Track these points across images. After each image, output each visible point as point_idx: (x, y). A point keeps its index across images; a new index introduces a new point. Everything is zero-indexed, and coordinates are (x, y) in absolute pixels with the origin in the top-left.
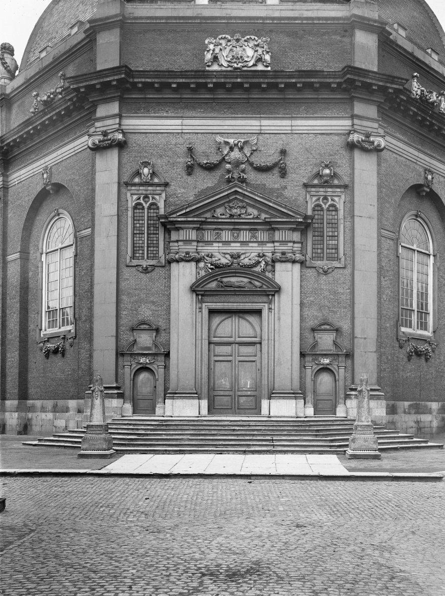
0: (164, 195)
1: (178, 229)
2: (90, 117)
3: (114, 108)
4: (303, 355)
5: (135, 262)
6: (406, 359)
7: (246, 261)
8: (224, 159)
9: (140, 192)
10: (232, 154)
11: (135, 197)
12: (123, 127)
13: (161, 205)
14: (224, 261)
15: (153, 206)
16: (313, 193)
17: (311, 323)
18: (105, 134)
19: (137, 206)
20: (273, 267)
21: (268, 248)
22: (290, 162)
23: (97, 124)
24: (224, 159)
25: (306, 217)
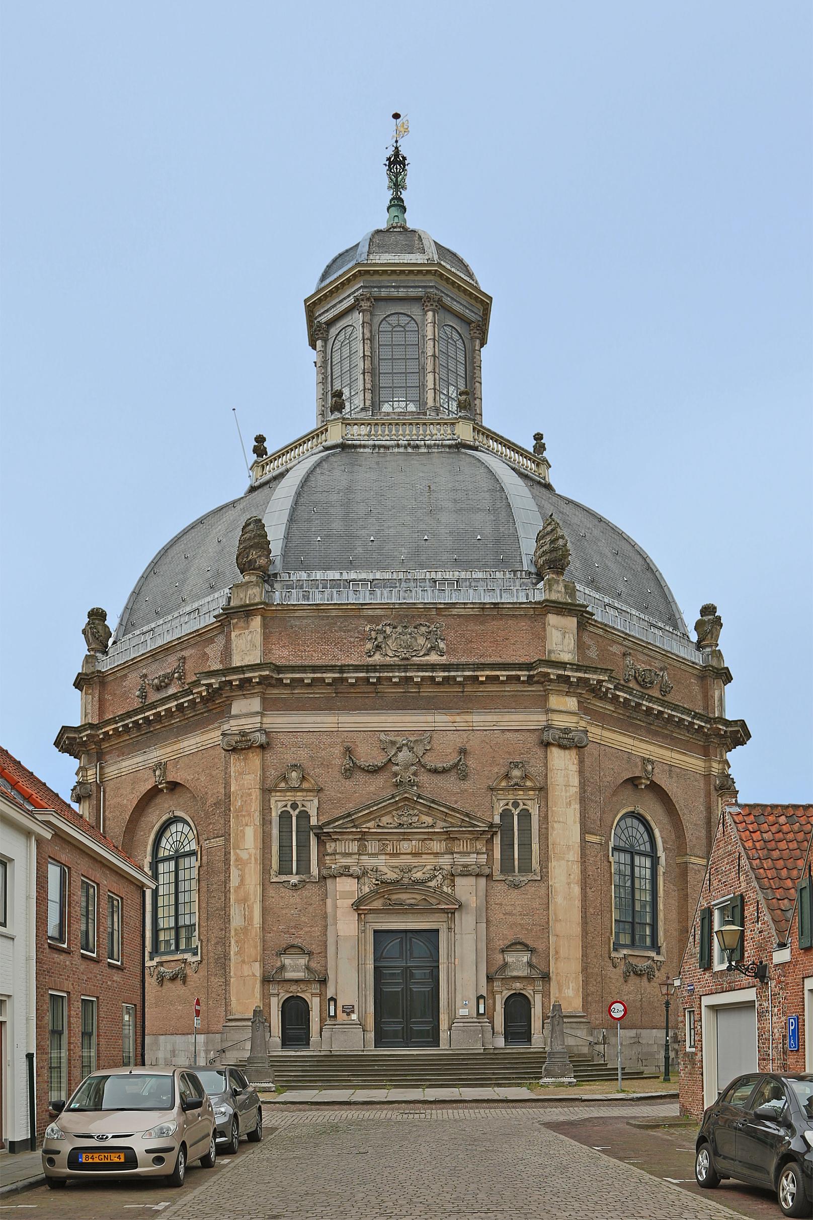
0: (316, 802)
1: (335, 840)
2: (224, 712)
3: (255, 704)
4: (490, 979)
5: (284, 878)
6: (622, 980)
7: (419, 875)
8: (390, 759)
9: (287, 798)
10: (400, 754)
11: (280, 804)
12: (264, 726)
13: (313, 812)
14: (391, 876)
15: (304, 816)
16: (499, 797)
17: (501, 944)
18: (243, 734)
19: (285, 817)
20: (453, 881)
21: (445, 861)
22: (472, 763)
23: (233, 722)
24: (390, 759)
25: (491, 825)
